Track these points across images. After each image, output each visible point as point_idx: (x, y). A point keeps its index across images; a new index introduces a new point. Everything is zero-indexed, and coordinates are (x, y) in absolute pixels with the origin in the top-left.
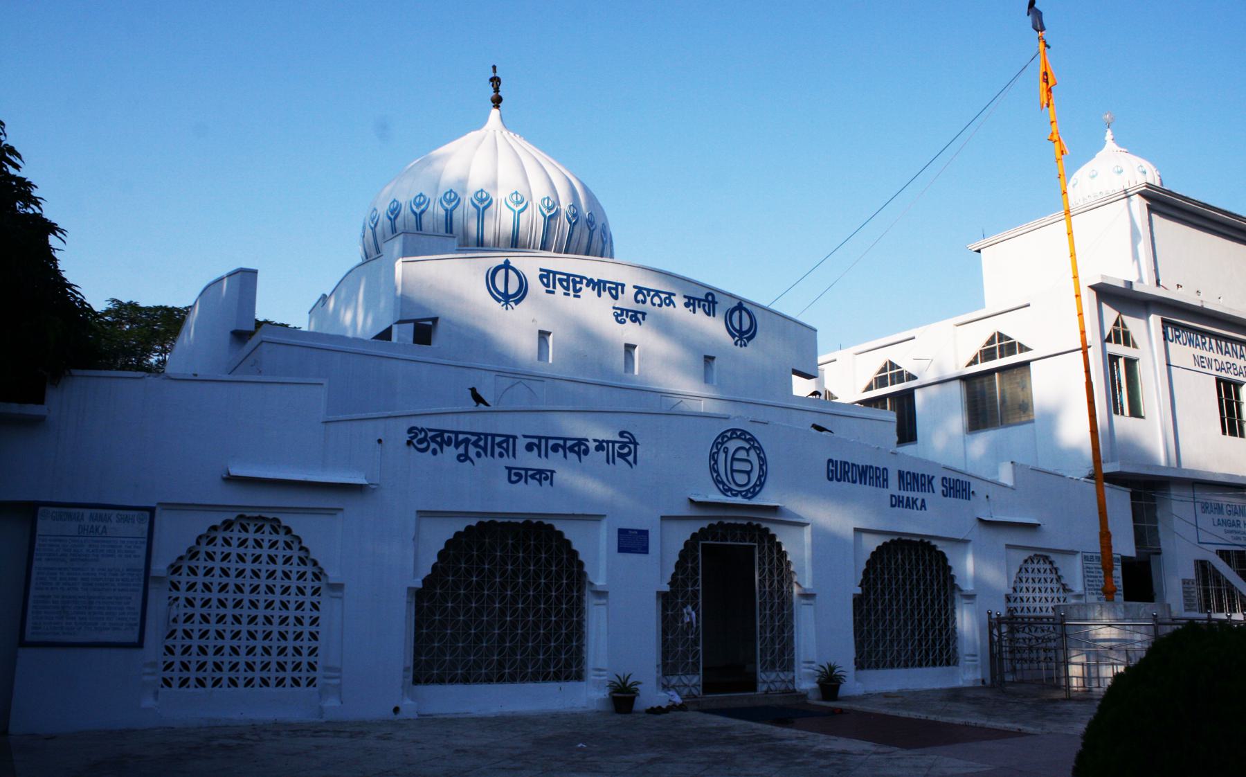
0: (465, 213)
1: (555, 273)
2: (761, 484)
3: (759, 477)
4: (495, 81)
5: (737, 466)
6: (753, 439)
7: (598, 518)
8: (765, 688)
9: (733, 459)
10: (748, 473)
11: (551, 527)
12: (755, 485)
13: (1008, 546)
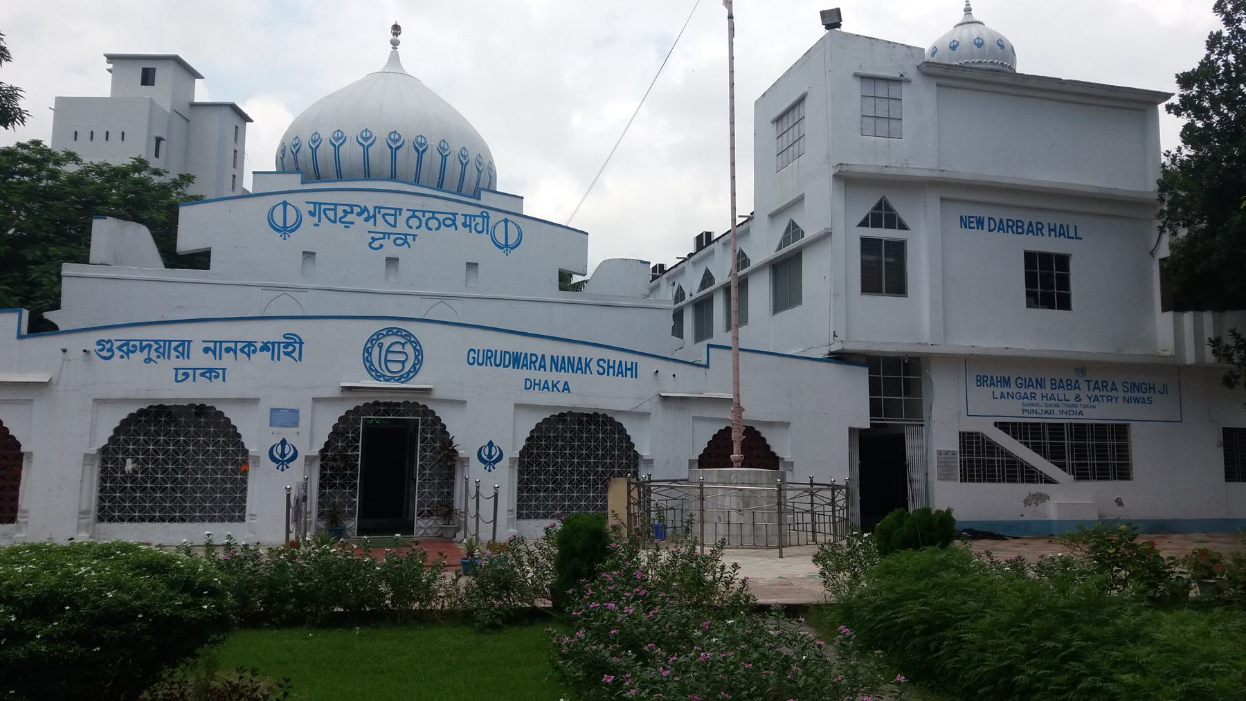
0: (326, 150)
1: (320, 204)
2: (415, 370)
3: (414, 365)
4: (396, 29)
5: (390, 357)
6: (410, 335)
7: (255, 401)
8: (421, 532)
9: (388, 351)
10: (403, 362)
11: (213, 408)
12: (410, 371)
13: (694, 418)
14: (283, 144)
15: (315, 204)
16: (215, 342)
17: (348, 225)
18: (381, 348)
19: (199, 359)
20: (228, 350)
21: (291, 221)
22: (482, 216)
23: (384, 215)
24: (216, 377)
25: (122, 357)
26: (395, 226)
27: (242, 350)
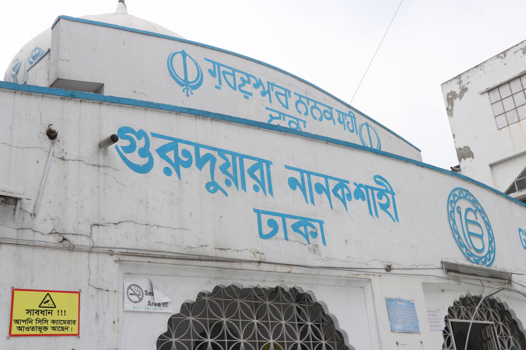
1: (219, 65)
14: (16, 59)
15: (214, 63)
16: (302, 172)
17: (248, 95)
18: (460, 213)
19: (287, 201)
20: (319, 188)
21: (192, 76)
22: (350, 116)
23: (277, 93)
24: (315, 235)
25: (167, 172)
26: (287, 107)
27: (335, 191)
